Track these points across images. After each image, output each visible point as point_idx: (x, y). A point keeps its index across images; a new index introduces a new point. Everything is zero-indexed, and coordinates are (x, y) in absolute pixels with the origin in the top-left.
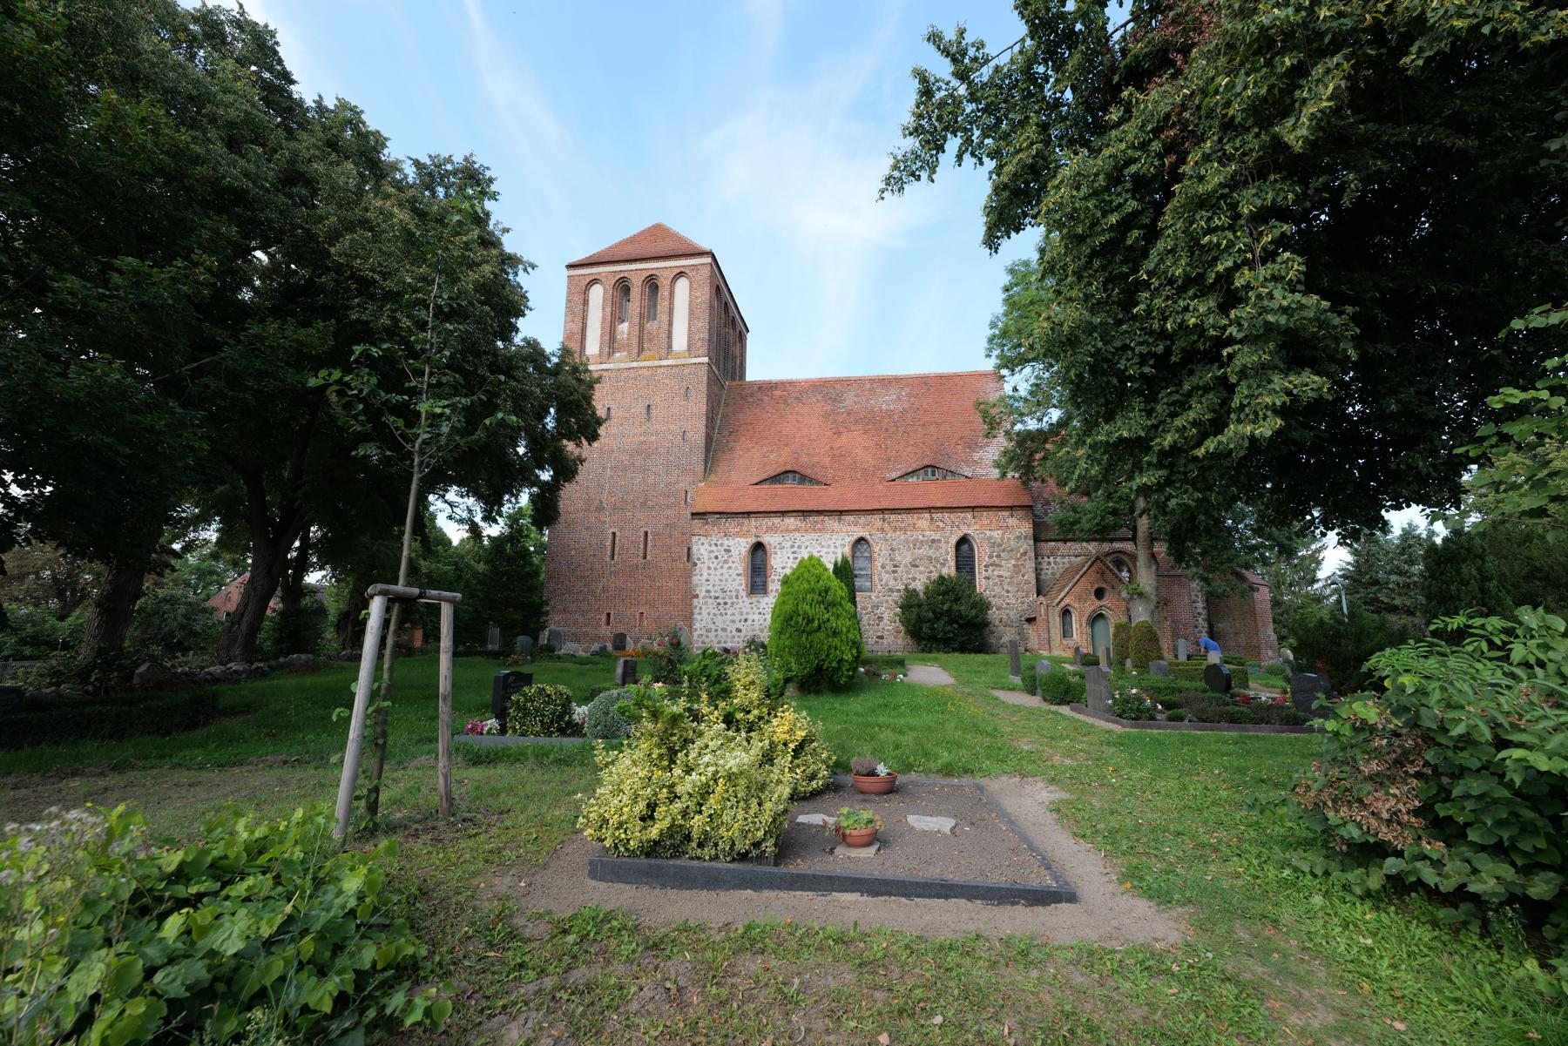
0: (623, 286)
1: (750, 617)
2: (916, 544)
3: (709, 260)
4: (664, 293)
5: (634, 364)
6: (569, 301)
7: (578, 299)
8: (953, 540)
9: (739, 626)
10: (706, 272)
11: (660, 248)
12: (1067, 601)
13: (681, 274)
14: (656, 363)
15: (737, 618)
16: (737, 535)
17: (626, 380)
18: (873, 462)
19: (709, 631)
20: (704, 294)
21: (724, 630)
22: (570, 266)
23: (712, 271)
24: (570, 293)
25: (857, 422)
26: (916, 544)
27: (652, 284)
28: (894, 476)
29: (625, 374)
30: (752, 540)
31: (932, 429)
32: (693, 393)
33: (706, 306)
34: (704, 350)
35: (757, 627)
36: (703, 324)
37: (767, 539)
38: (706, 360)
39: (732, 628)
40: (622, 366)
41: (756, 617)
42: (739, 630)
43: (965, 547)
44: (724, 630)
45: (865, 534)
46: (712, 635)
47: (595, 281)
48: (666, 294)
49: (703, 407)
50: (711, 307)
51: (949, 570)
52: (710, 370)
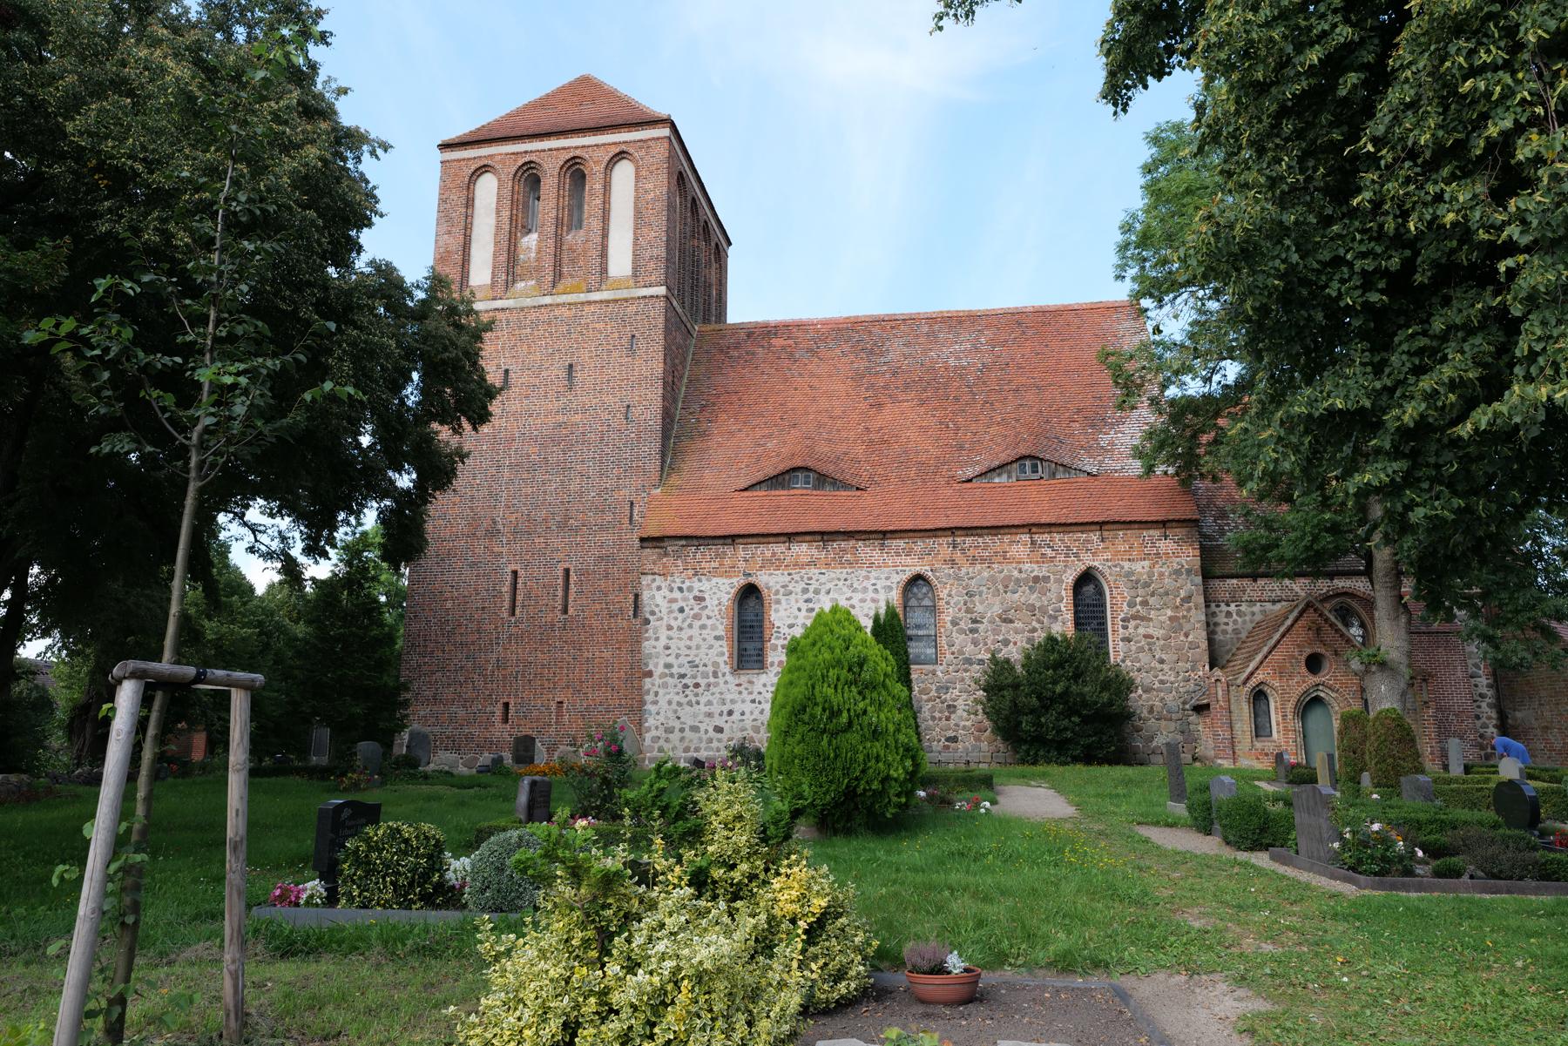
0: (529, 176)
1: (737, 708)
2: (1008, 585)
3: (666, 132)
4: (594, 184)
5: (548, 300)
6: (443, 201)
7: (457, 197)
8: (1070, 578)
9: (720, 722)
10: (661, 151)
11: (589, 114)
12: (1260, 676)
13: (621, 155)
14: (583, 297)
15: (716, 709)
16: (715, 573)
17: (534, 325)
18: (934, 451)
19: (670, 730)
20: (659, 185)
21: (695, 729)
22: (445, 146)
24: (444, 188)
25: (907, 386)
26: (1008, 585)
27: (575, 171)
28: (970, 473)
29: (533, 316)
30: (739, 581)
31: (1030, 396)
33: (661, 205)
34: (659, 275)
35: (748, 723)
36: (657, 234)
37: (763, 579)
38: (662, 290)
39: (707, 726)
40: (529, 302)
41: (748, 707)
42: (719, 730)
43: (1089, 589)
44: (695, 729)
45: (924, 569)
46: (675, 737)
47: (484, 169)
48: (598, 186)
49: (659, 368)
50: (670, 206)
51: (1064, 626)
52: (669, 307)
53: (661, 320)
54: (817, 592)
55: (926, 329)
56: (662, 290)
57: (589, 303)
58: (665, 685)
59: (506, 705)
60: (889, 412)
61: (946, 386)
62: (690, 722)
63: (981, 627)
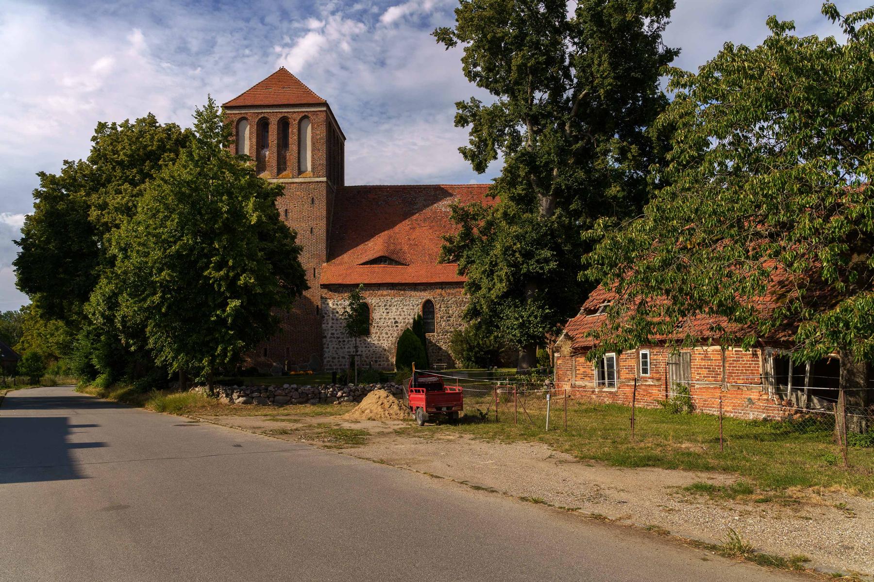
0: (263, 125)
3: (325, 109)
4: (293, 130)
10: (322, 117)
14: (290, 180)
19: (334, 358)
20: (322, 132)
21: (343, 358)
23: (327, 116)
25: (425, 220)
27: (284, 123)
32: (316, 202)
33: (324, 141)
34: (323, 171)
38: (324, 179)
41: (364, 349)
45: (430, 297)
46: (336, 361)
49: (324, 213)
52: (328, 186)
53: (325, 192)
54: (390, 306)
55: (433, 193)
56: (324, 179)
57: (293, 183)
58: (331, 341)
59: (266, 349)
60: (418, 232)
61: (441, 220)
62: (342, 355)
63: (452, 319)
